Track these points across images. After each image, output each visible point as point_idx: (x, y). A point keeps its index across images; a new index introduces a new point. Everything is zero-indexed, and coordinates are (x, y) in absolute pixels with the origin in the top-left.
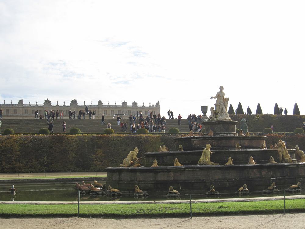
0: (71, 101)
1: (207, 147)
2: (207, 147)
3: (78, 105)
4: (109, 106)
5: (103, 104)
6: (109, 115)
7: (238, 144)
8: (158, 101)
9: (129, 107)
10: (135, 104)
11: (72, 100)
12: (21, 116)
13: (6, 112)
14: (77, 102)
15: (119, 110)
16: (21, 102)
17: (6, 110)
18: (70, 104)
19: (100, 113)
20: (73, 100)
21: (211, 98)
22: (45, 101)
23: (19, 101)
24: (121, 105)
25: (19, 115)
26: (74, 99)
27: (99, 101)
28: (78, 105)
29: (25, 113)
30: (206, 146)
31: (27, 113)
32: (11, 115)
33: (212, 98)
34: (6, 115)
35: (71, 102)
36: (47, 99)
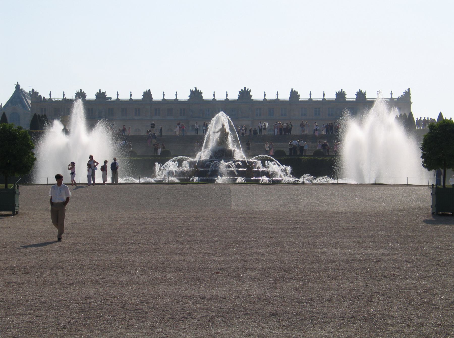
0: (240, 92)
3: (252, 98)
5: (299, 96)
8: (409, 90)
11: (242, 90)
14: (251, 94)
16: (148, 94)
18: (237, 97)
20: (244, 89)
22: (192, 91)
23: (144, 93)
26: (245, 88)
27: (292, 90)
28: (252, 98)
35: (239, 94)
36: (196, 88)
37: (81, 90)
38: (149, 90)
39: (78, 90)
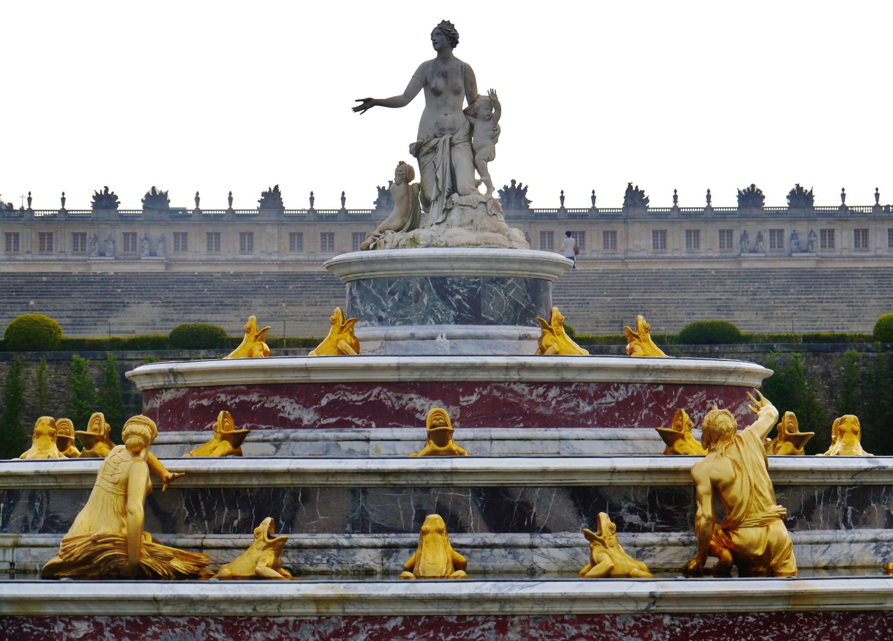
1: (127, 436)
2: (127, 436)
3: (532, 206)
4: (675, 208)
5: (647, 200)
6: (676, 254)
7: (438, 413)
9: (777, 214)
10: (800, 197)
11: (506, 187)
12: (273, 263)
13: (205, 244)
14: (528, 196)
15: (725, 226)
16: (272, 198)
17: (205, 237)
19: (636, 242)
20: (510, 186)
21: (356, 110)
23: (264, 194)
24: (734, 203)
25: (264, 257)
26: (513, 182)
27: (630, 186)
28: (532, 206)
29: (292, 248)
30: (121, 429)
31: (300, 248)
32: (230, 257)
33: (368, 104)
34: (204, 258)
37: (107, 188)
38: (277, 187)
39: (100, 189)
